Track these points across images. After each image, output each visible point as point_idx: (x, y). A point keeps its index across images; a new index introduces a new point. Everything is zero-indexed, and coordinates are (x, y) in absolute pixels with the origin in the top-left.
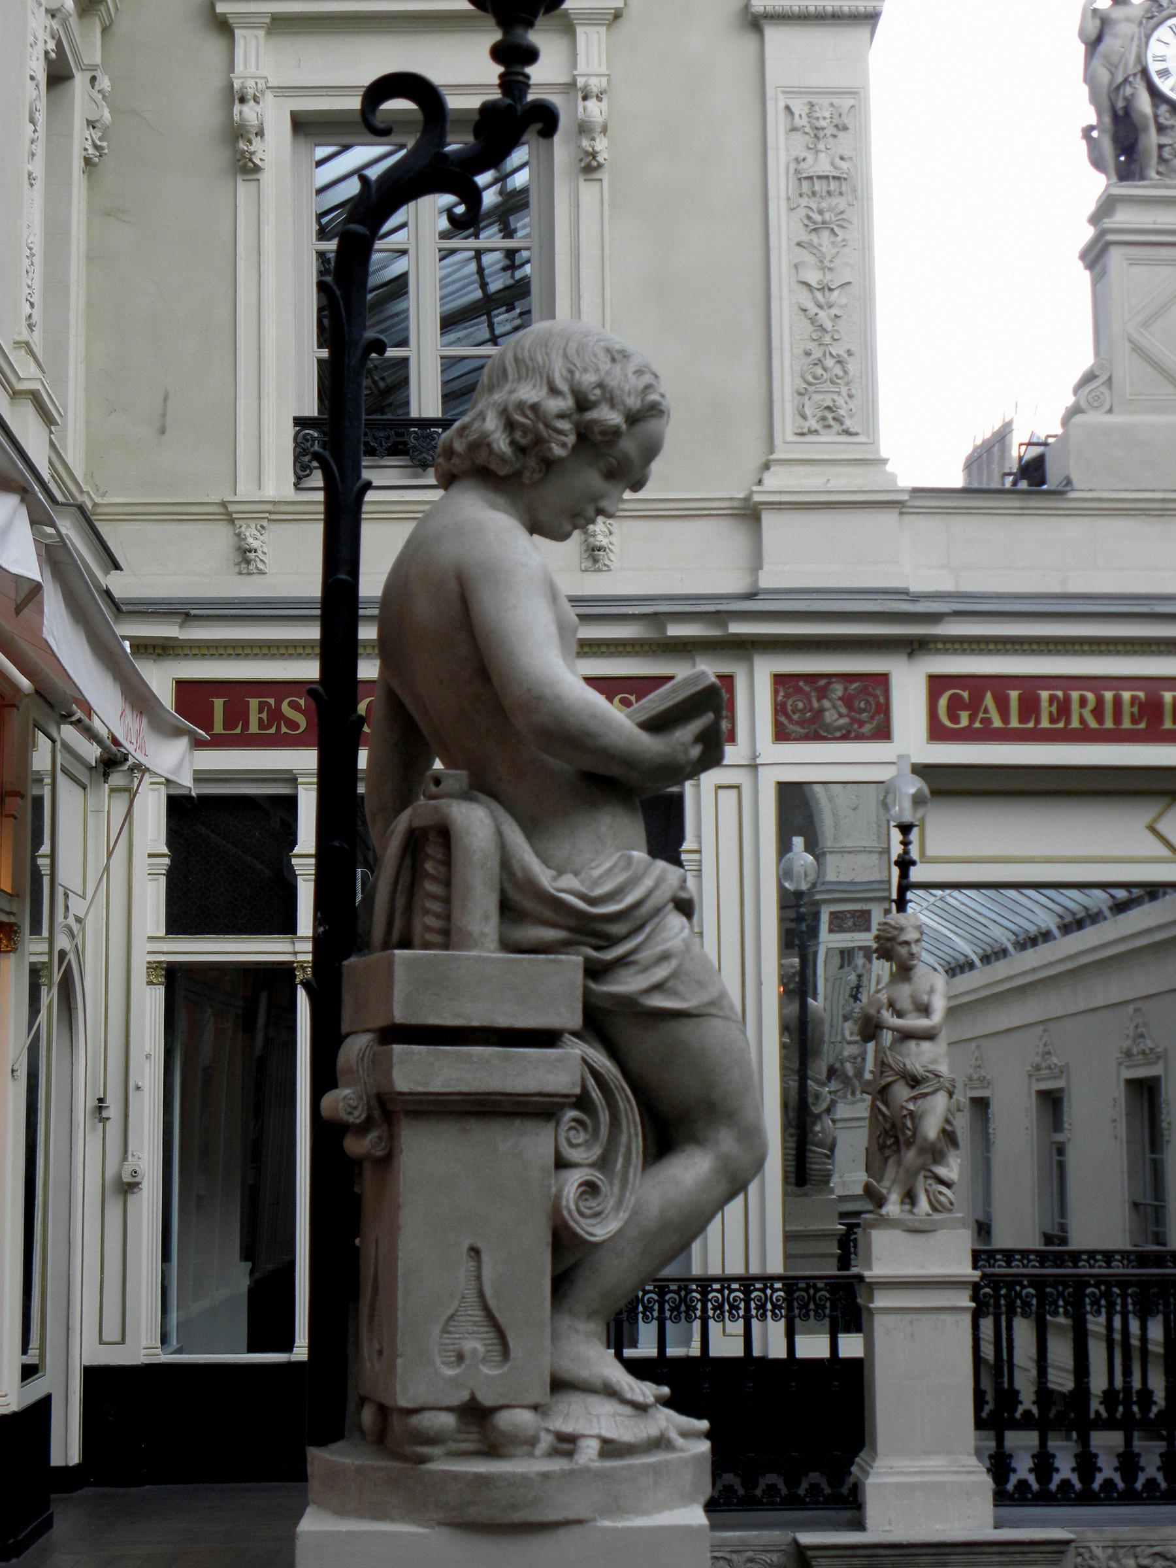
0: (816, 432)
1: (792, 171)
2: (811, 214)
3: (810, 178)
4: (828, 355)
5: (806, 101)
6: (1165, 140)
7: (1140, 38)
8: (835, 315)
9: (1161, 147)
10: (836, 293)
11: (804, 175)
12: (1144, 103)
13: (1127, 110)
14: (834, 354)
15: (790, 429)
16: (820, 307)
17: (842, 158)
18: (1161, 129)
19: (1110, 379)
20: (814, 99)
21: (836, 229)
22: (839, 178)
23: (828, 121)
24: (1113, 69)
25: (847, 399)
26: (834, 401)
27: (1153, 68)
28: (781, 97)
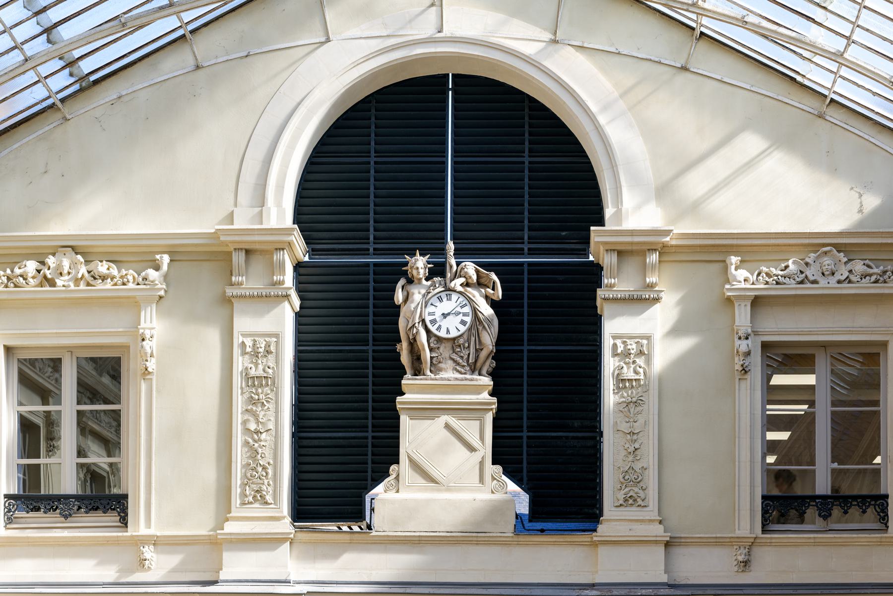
0: (251, 503)
1: (244, 374)
2: (253, 395)
3: (254, 377)
4: (259, 465)
5: (253, 339)
6: (434, 355)
7: (422, 304)
8: (263, 445)
9: (432, 358)
10: (264, 434)
11: (250, 376)
12: (423, 336)
13: (415, 339)
14: (262, 464)
15: (238, 502)
16: (255, 441)
17: (269, 368)
18: (431, 350)
19: (398, 475)
20: (257, 339)
21: (265, 403)
22: (267, 377)
23: (263, 348)
24: (409, 319)
25: (268, 486)
26: (260, 487)
27: (428, 319)
28: (241, 337)
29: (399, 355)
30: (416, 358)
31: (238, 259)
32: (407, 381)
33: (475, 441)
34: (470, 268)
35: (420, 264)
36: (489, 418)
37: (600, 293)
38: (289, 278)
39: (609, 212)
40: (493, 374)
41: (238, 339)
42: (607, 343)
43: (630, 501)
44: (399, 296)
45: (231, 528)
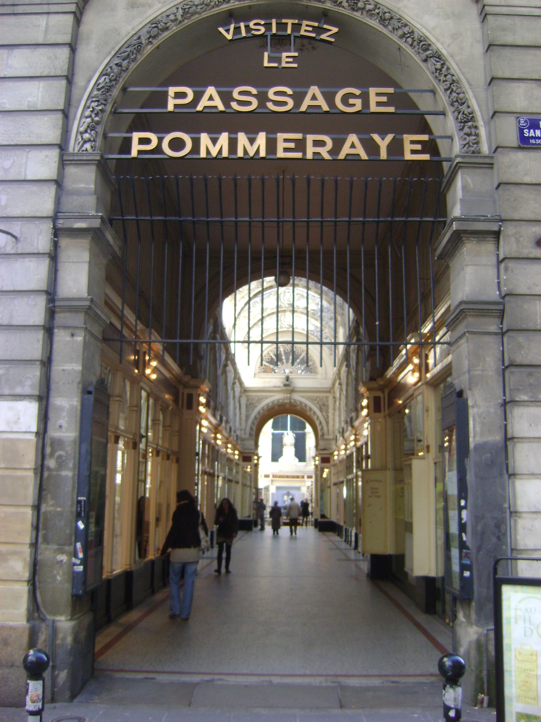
35: (285, 432)
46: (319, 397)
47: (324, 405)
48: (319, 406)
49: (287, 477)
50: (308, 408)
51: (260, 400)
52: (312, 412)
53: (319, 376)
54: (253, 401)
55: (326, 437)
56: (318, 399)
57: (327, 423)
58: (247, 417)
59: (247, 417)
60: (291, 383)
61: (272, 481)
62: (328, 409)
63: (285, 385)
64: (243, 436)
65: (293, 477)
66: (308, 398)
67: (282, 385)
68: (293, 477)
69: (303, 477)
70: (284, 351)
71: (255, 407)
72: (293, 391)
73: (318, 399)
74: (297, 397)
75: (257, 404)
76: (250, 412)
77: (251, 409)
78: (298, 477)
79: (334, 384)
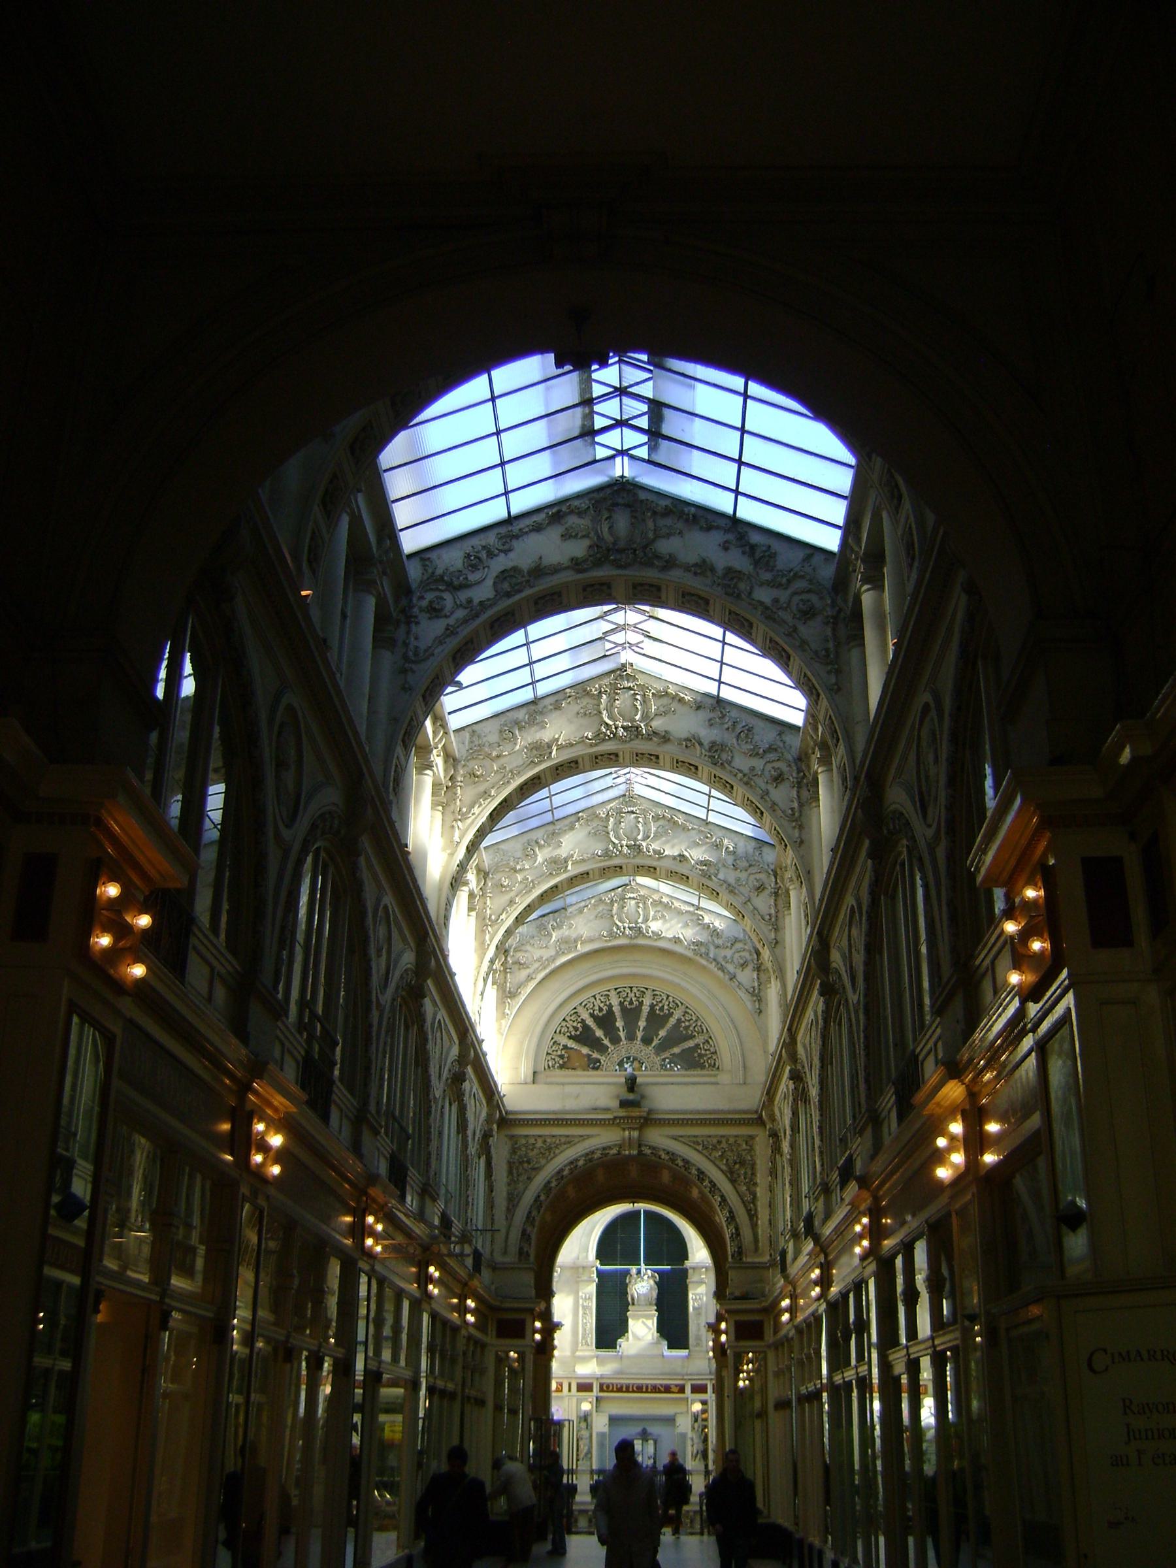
29: (627, 1298)
30: (633, 1299)
31: (581, 1270)
32: (630, 1308)
33: (651, 1326)
34: (649, 1272)
35: (634, 1269)
36: (655, 1319)
37: (688, 1281)
38: (595, 1275)
39: (690, 1258)
40: (656, 1305)
41: (580, 1294)
42: (690, 1296)
43: (698, 1345)
44: (627, 1281)
45: (578, 1353)
46: (727, 1137)
47: (742, 1163)
48: (727, 1164)
49: (639, 1389)
50: (694, 1172)
51: (550, 1150)
52: (706, 1183)
53: (723, 1078)
54: (531, 1154)
55: (749, 1259)
56: (724, 1145)
57: (752, 1216)
58: (513, 1200)
59: (513, 1200)
60: (643, 1097)
61: (597, 1398)
62: (753, 1174)
63: (624, 1104)
64: (499, 1258)
65: (655, 1389)
66: (693, 1142)
67: (615, 1104)
68: (655, 1389)
69: (682, 1389)
70: (621, 1004)
71: (537, 1170)
72: (648, 1121)
73: (724, 1145)
74: (658, 1138)
75: (543, 1161)
76: (521, 1186)
77: (524, 1177)
78: (667, 1389)
79: (770, 1091)
